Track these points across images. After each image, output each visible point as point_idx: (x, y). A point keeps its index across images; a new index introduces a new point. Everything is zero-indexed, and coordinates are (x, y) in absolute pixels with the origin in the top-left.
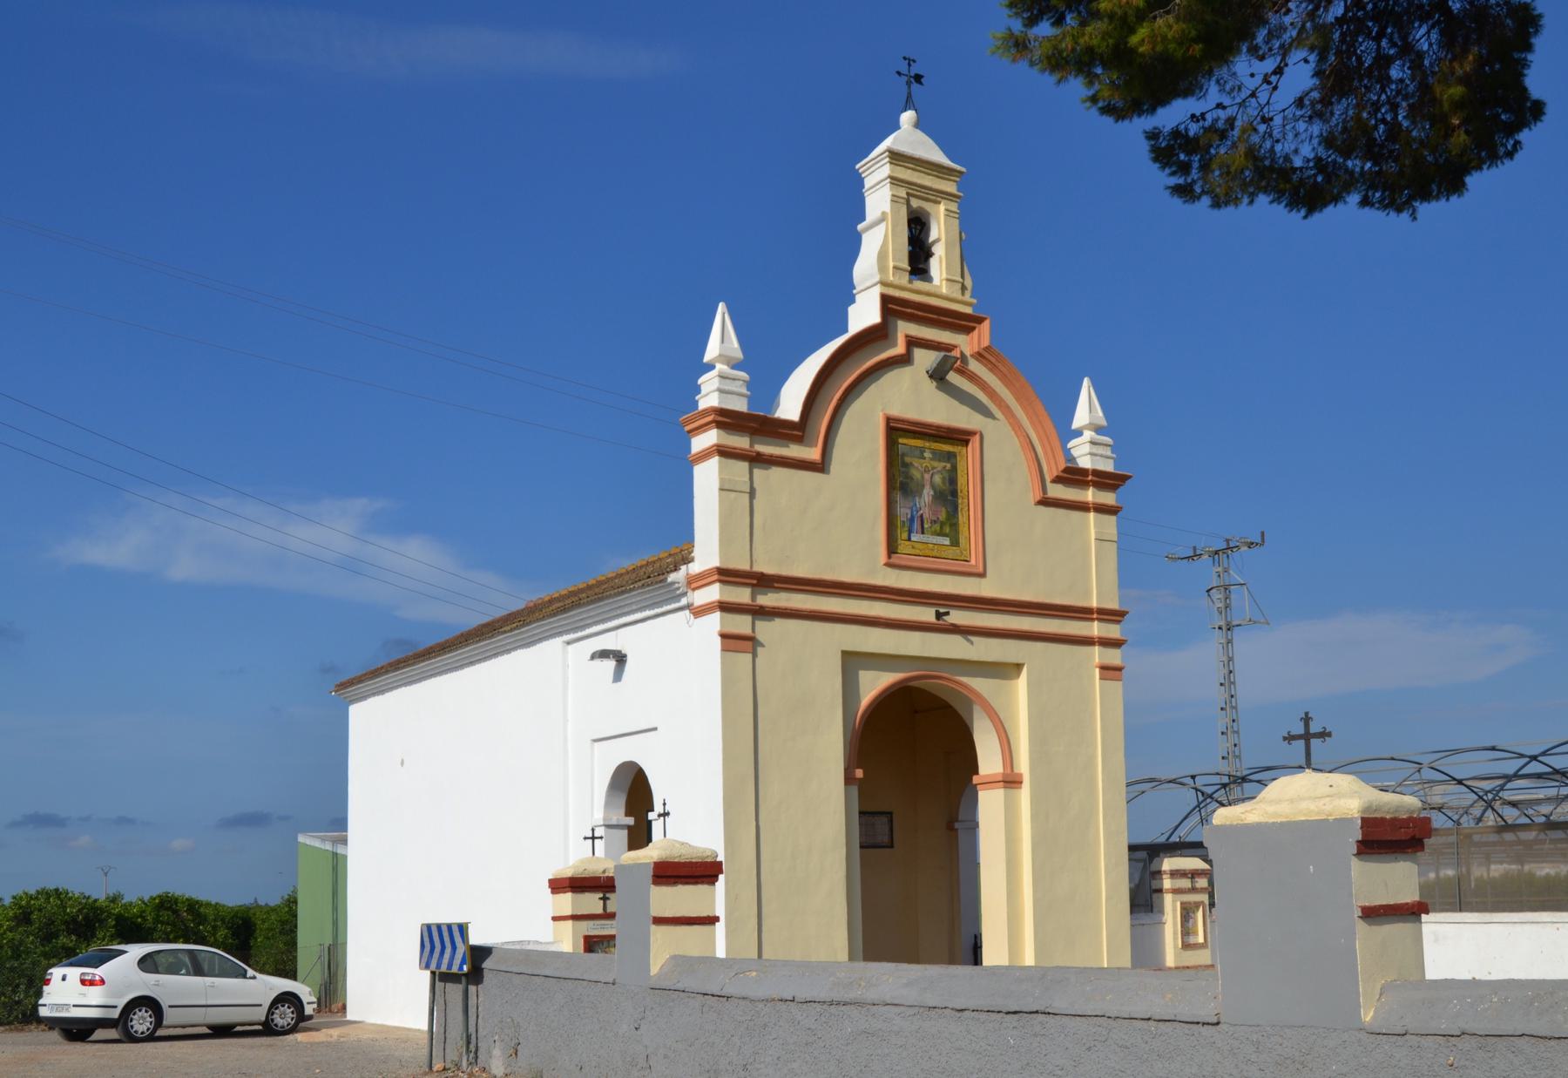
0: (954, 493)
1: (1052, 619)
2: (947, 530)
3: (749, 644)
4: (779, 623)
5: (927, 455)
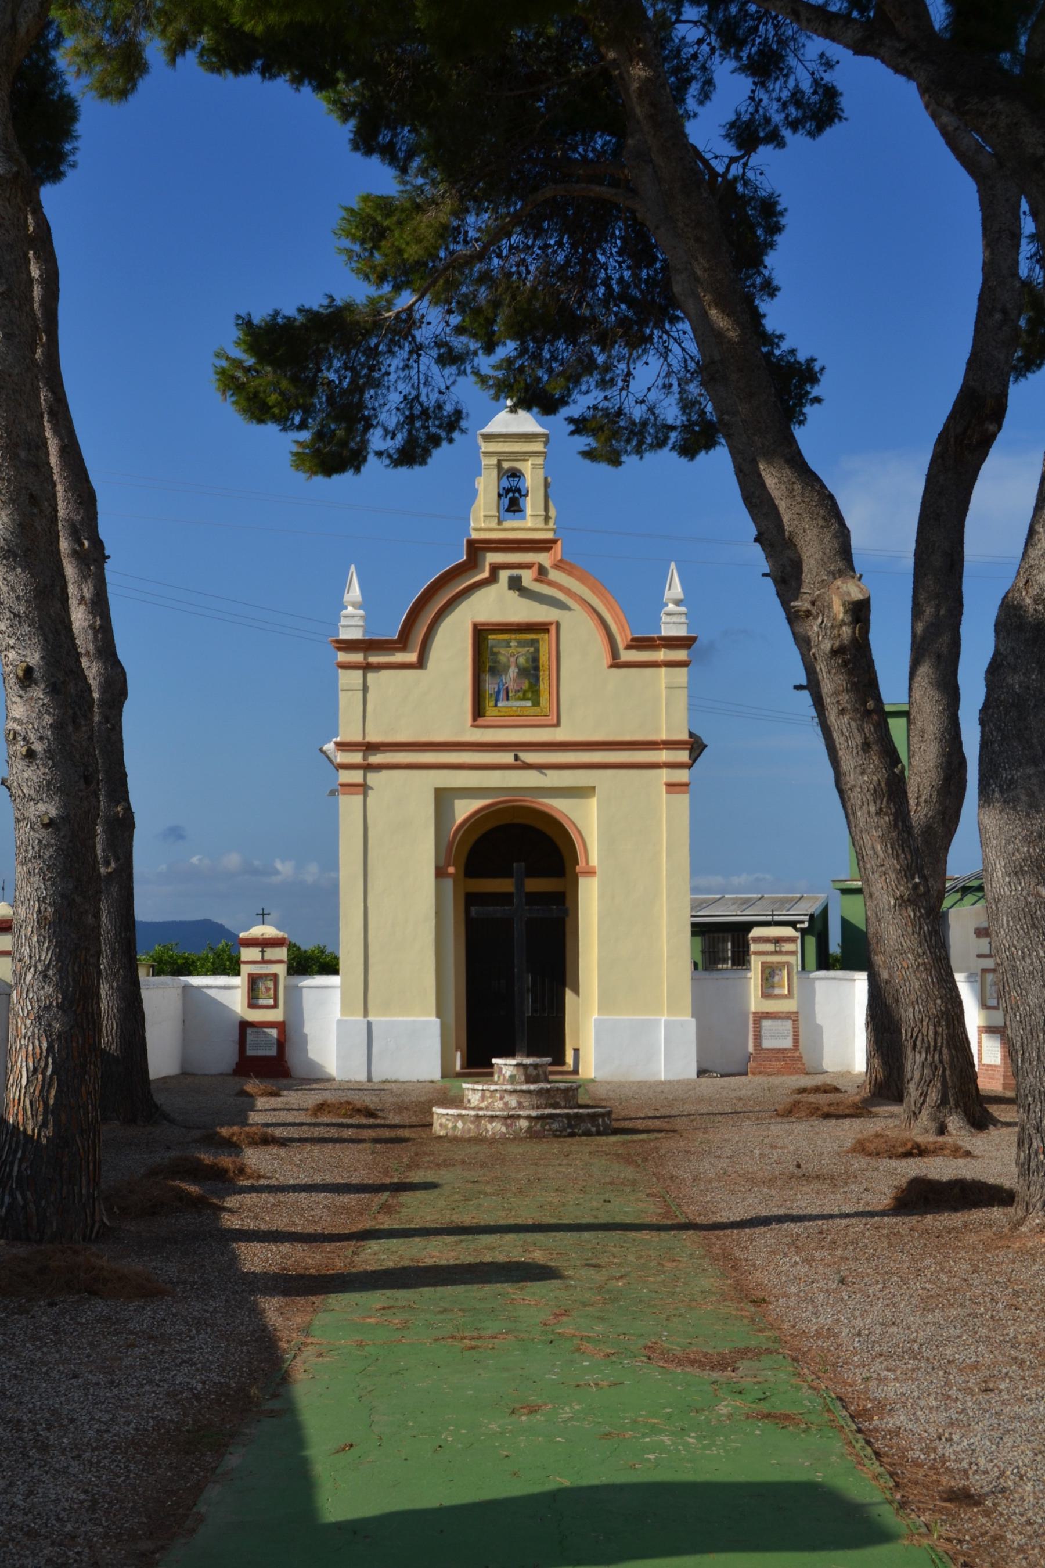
0: (537, 668)
1: (624, 752)
2: (529, 695)
3: (361, 789)
4: (385, 773)
5: (513, 644)
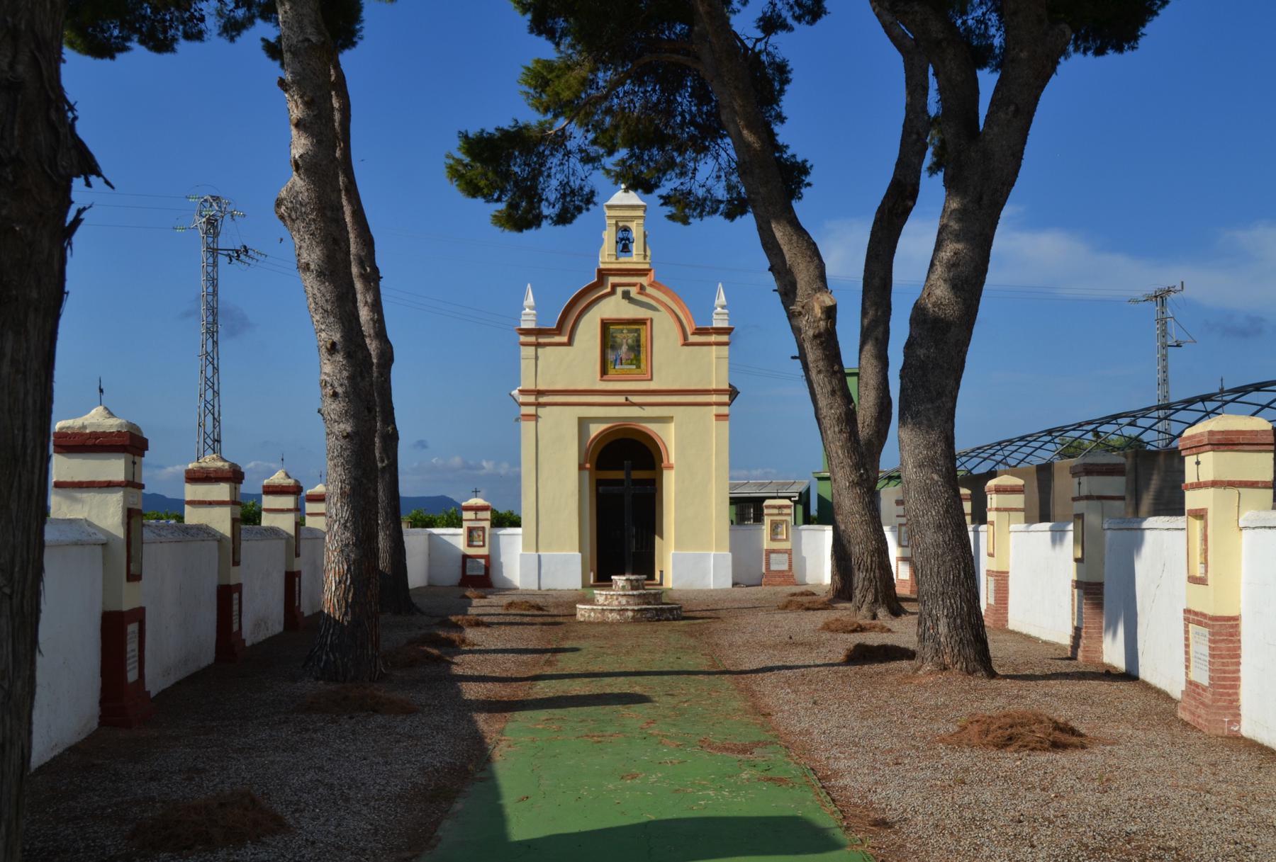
0: (639, 346)
